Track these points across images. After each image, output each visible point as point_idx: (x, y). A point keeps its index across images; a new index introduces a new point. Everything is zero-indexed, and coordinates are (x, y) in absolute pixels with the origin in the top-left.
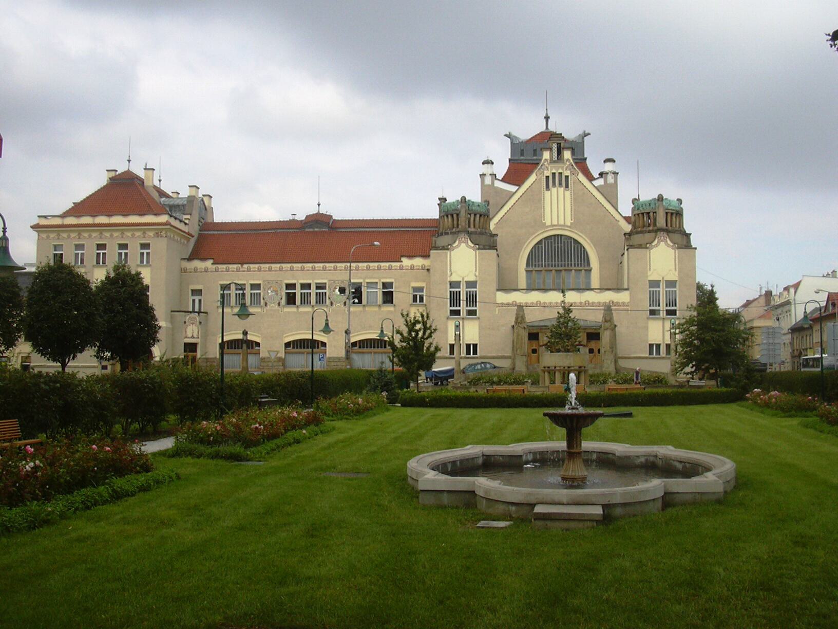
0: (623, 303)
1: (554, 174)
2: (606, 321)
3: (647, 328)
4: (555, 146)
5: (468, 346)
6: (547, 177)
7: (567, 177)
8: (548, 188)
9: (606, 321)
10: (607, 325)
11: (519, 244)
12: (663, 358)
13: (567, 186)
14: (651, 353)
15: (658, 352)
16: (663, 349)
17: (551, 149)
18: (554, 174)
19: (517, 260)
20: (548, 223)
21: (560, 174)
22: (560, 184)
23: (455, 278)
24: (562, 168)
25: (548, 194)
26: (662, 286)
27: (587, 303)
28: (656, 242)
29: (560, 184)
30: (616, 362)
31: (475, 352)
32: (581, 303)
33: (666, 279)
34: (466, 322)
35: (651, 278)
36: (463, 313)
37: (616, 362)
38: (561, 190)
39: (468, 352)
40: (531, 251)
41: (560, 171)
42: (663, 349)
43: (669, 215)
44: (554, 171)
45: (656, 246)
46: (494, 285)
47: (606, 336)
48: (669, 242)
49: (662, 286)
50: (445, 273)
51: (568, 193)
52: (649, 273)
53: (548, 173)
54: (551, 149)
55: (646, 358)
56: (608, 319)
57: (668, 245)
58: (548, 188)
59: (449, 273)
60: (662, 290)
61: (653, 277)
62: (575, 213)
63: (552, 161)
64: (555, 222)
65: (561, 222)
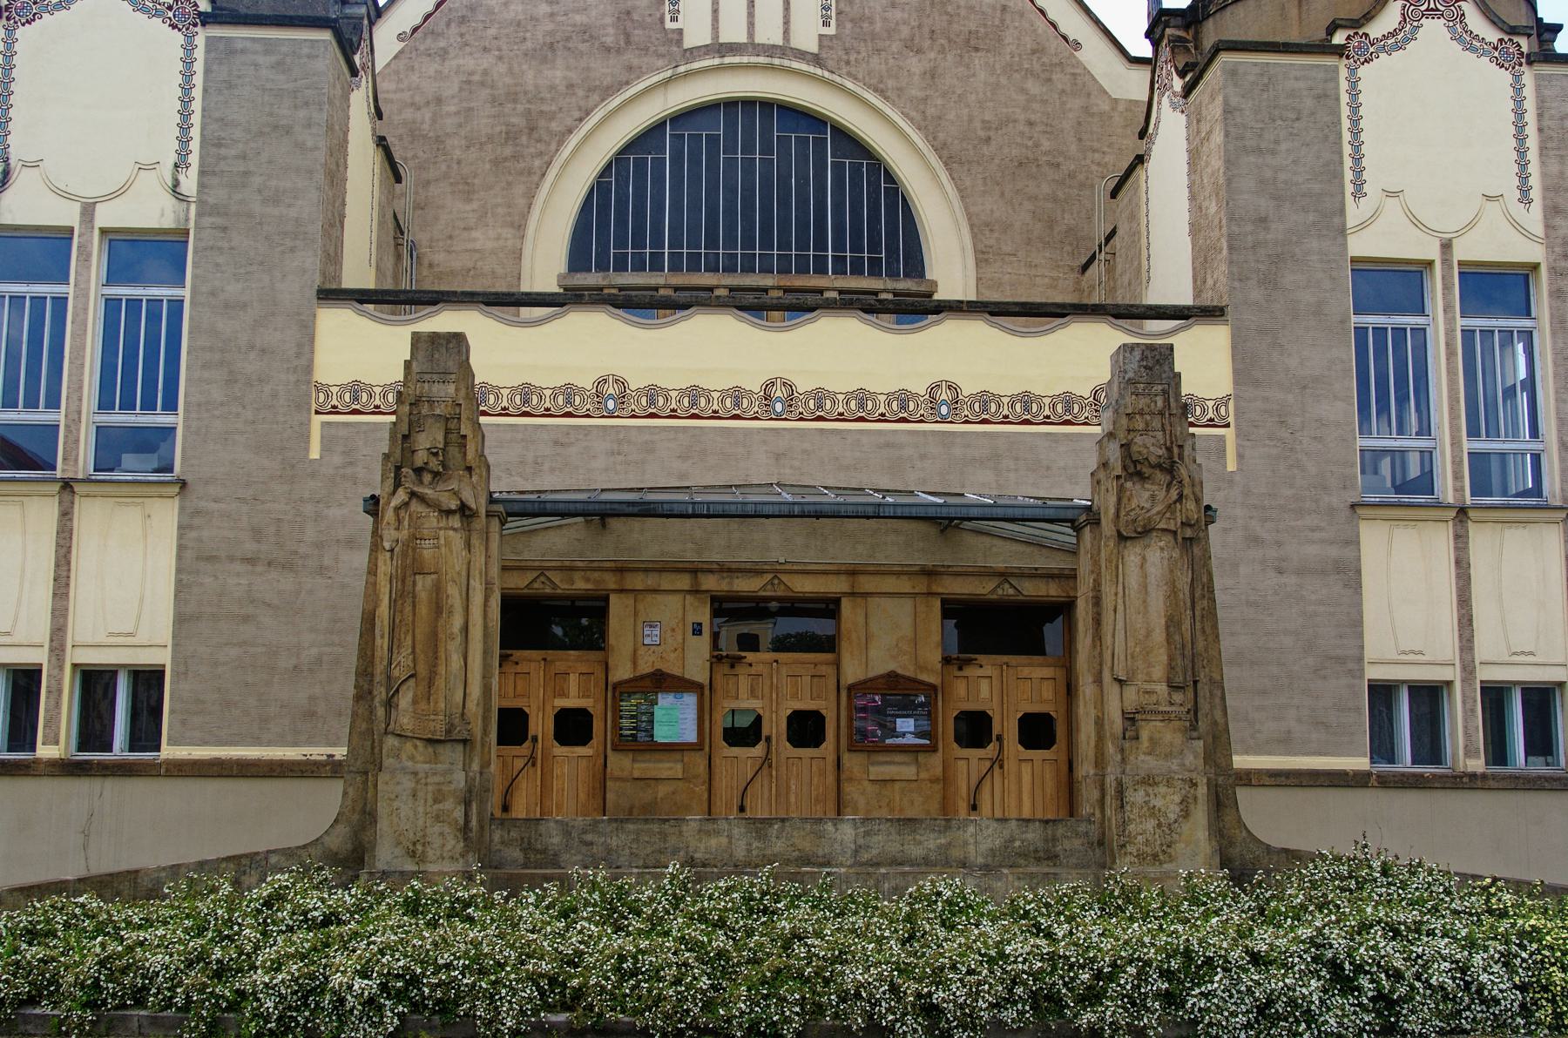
2: (1135, 469)
3: (1350, 575)
9: (1135, 469)
10: (1146, 498)
12: (1468, 782)
14: (1382, 747)
15: (1430, 744)
16: (1463, 728)
19: (520, 227)
20: (697, 33)
26: (1441, 294)
27: (943, 401)
30: (1221, 802)
31: (146, 732)
33: (1466, 251)
34: (91, 514)
35: (1361, 245)
37: (1221, 802)
39: (93, 731)
40: (600, 188)
42: (1463, 728)
45: (1397, 40)
47: (1133, 595)
48: (1475, 21)
49: (1441, 294)
52: (1354, 213)
56: (1150, 446)
57: (1469, 42)
60: (1442, 320)
61: (1378, 235)
64: (734, 32)
65: (769, 33)
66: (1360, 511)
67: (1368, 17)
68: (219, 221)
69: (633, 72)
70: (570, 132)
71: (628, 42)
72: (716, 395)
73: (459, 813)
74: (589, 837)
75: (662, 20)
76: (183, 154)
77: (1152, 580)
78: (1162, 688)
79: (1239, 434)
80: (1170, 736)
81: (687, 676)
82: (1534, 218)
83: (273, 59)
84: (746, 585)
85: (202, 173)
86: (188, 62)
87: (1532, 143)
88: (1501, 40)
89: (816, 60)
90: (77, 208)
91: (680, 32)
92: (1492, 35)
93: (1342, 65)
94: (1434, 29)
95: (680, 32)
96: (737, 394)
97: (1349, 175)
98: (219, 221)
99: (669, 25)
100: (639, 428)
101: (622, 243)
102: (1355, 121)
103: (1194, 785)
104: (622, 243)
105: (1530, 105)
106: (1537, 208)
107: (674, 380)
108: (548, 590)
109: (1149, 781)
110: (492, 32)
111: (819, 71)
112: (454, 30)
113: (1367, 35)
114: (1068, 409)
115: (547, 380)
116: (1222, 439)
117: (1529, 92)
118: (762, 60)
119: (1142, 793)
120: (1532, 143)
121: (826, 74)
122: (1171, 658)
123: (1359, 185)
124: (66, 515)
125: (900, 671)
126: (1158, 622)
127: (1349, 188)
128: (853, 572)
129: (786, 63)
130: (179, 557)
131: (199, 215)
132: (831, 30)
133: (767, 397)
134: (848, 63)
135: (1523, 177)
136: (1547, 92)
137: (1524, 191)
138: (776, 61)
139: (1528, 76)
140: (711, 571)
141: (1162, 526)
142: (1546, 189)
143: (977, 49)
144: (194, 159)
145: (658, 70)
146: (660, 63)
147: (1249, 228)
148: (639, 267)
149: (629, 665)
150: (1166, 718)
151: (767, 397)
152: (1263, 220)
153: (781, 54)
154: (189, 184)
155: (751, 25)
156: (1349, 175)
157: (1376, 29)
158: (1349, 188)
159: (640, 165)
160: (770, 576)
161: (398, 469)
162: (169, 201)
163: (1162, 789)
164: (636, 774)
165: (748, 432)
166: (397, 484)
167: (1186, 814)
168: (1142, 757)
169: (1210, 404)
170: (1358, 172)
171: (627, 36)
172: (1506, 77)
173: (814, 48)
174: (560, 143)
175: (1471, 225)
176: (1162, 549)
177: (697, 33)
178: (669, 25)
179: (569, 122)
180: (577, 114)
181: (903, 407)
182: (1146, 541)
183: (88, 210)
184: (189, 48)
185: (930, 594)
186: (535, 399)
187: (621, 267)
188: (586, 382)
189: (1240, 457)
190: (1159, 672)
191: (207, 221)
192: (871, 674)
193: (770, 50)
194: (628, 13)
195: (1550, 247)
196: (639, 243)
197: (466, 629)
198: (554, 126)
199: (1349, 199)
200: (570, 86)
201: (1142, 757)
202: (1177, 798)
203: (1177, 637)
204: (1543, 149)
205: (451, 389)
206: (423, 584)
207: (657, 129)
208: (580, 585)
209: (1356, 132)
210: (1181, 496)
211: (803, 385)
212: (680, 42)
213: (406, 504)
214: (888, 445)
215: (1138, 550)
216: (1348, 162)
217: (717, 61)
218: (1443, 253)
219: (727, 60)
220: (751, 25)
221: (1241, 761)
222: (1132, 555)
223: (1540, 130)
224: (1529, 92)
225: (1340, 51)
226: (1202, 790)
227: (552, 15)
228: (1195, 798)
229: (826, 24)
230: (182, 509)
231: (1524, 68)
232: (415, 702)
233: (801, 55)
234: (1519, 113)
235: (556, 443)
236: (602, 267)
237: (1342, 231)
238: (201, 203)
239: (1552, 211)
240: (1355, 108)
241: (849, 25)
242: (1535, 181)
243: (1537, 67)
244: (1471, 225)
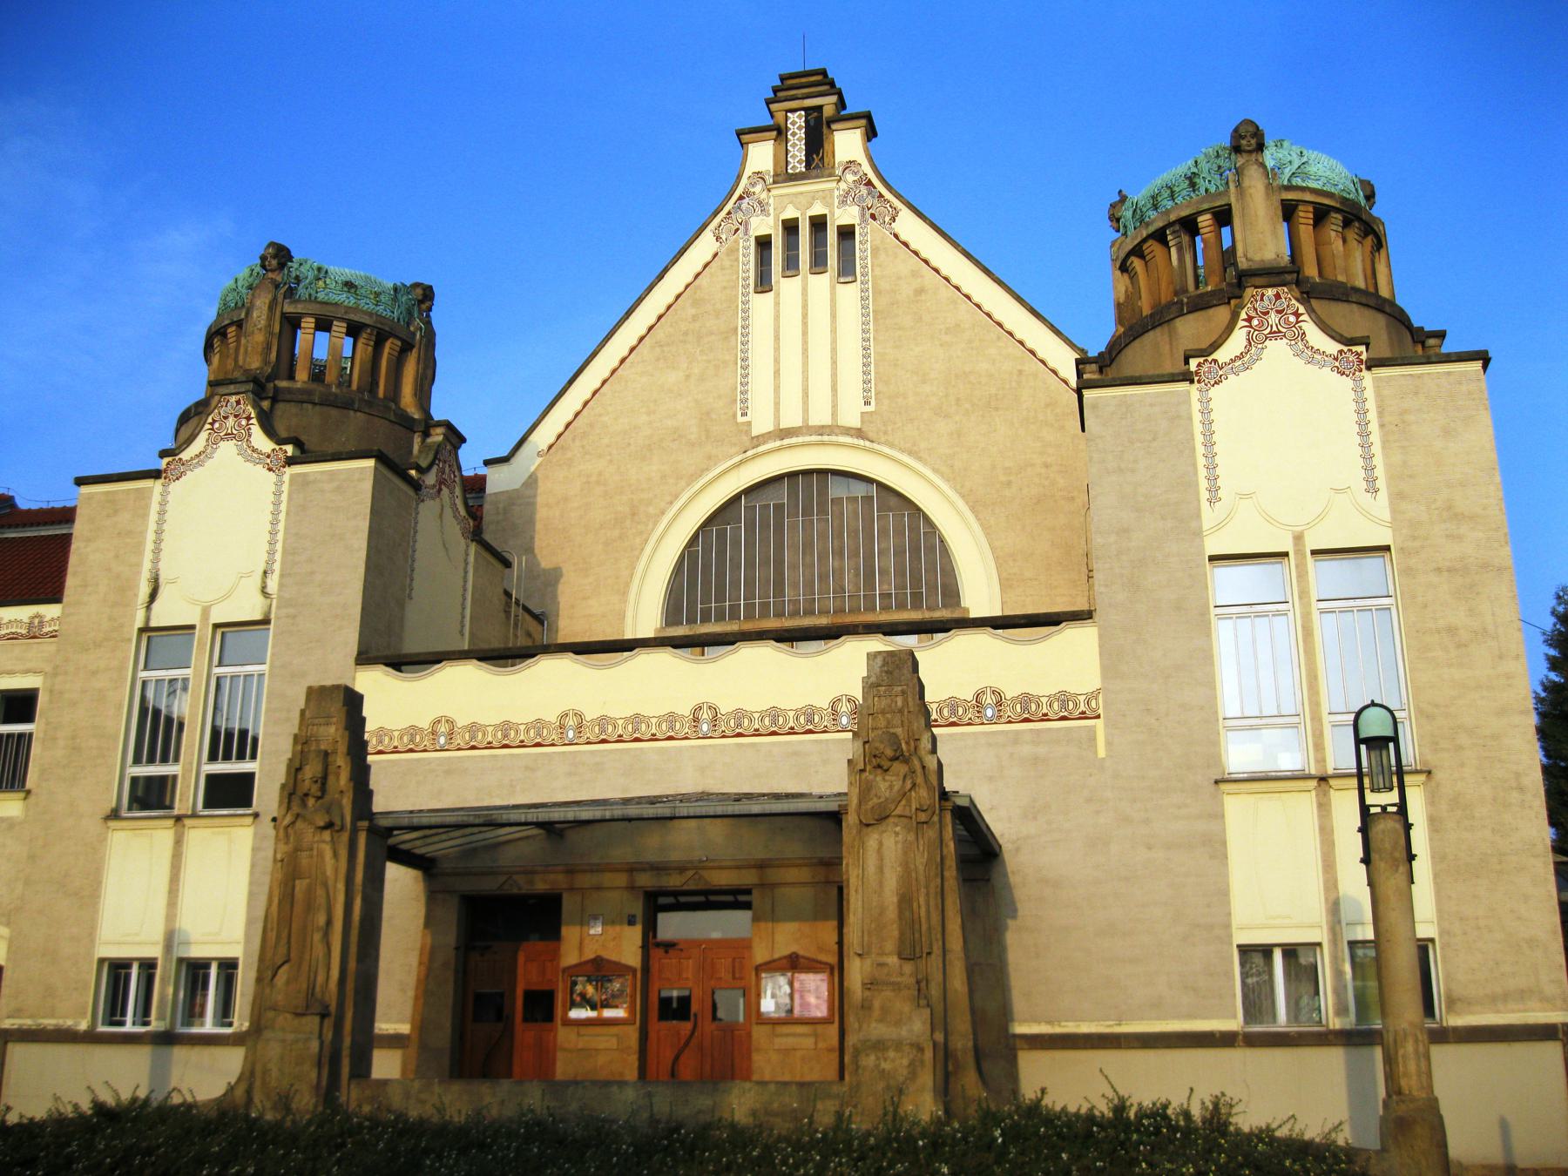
0: (1064, 698)
1: (790, 228)
3: (1216, 847)
4: (797, 122)
5: (195, 971)
6: (764, 243)
7: (846, 233)
8: (764, 283)
10: (886, 786)
11: (633, 524)
13: (847, 269)
17: (780, 132)
18: (790, 228)
19: (624, 593)
21: (819, 224)
22: (819, 263)
23: (166, 613)
24: (826, 197)
25: (761, 304)
28: (1237, 341)
29: (819, 263)
32: (810, 713)
36: (189, 794)
38: (821, 284)
41: (818, 209)
43: (1305, 216)
44: (790, 213)
45: (1242, 361)
46: (349, 638)
50: (125, 588)
51: (849, 294)
53: (766, 225)
54: (780, 132)
55: (1225, 1040)
57: (1312, 355)
58: (764, 283)
59: (144, 590)
62: (878, 377)
63: (784, 176)
64: (791, 419)
65: (820, 417)
66: (1224, 787)
67: (1215, 346)
68: (291, 611)
69: (712, 460)
70: (663, 513)
71: (708, 437)
72: (654, 721)
73: (314, 1075)
74: (423, 1096)
75: (735, 416)
76: (270, 562)
77: (887, 862)
78: (893, 960)
79: (1106, 725)
80: (903, 1006)
81: (623, 961)
82: (1381, 505)
83: (335, 484)
84: (674, 881)
85: (282, 576)
86: (278, 494)
87: (1375, 438)
88: (1341, 352)
89: (859, 433)
90: (198, 610)
91: (749, 423)
92: (1333, 347)
93: (1194, 390)
94: (1277, 350)
95: (749, 423)
96: (671, 718)
97: (1203, 485)
98: (291, 611)
99: (740, 419)
100: (592, 752)
101: (706, 599)
102: (1208, 434)
103: (921, 1049)
104: (706, 599)
105: (1371, 405)
106: (1383, 495)
107: (620, 710)
108: (515, 891)
109: (879, 1046)
110: (606, 441)
111: (861, 442)
112: (578, 443)
113: (1215, 361)
114: (954, 711)
115: (522, 716)
116: (1092, 730)
117: (1369, 394)
118: (815, 438)
119: (873, 1057)
120: (1375, 438)
121: (867, 444)
122: (902, 934)
123: (1214, 490)
124: (178, 842)
125: (801, 953)
126: (891, 898)
127: (1204, 495)
128: (762, 866)
129: (833, 438)
130: (252, 873)
131: (278, 607)
132: (871, 408)
133: (696, 720)
134: (885, 433)
135: (1369, 469)
136: (1385, 392)
137: (1371, 482)
138: (826, 438)
139: (1368, 377)
140: (644, 870)
141: (897, 812)
142: (1391, 478)
143: (997, 409)
144: (277, 566)
145: (731, 457)
146: (734, 450)
147: (1113, 538)
148: (720, 617)
149: (576, 953)
150: (897, 987)
151: (696, 720)
152: (1124, 531)
153: (827, 432)
154: (273, 585)
155: (806, 411)
156: (1203, 485)
157: (1222, 355)
158: (1204, 495)
159: (722, 536)
160: (691, 873)
161: (290, 795)
162: (260, 598)
163: (891, 1054)
164: (580, 1045)
165: (680, 749)
166: (289, 808)
167: (913, 1075)
168: (874, 1025)
169: (1082, 698)
170: (1213, 478)
171: (707, 431)
172: (1347, 382)
173: (856, 423)
174: (655, 524)
175: (1321, 517)
176: (897, 834)
177: (762, 422)
178: (740, 419)
179: (663, 505)
180: (668, 499)
181: (810, 721)
182: (883, 827)
183: (206, 612)
184: (279, 484)
185: (827, 882)
186: (512, 733)
187: (706, 618)
188: (552, 717)
189: (1109, 744)
190: (890, 946)
191: (284, 611)
192: (776, 956)
193: (820, 430)
194: (708, 414)
195: (1396, 530)
196: (720, 598)
197: (329, 922)
198: (651, 510)
199: (1204, 505)
200: (664, 477)
201: (874, 1025)
202: (905, 1062)
203: (907, 914)
204: (1385, 444)
205: (332, 729)
206: (301, 886)
207: (735, 499)
208: (541, 886)
209: (1209, 444)
210: (914, 785)
211: (725, 708)
212: (748, 432)
213: (293, 823)
214: (796, 754)
215: (876, 836)
216: (1202, 473)
217: (778, 443)
218: (1295, 545)
219: (786, 442)
220: (806, 411)
221: (1020, 1029)
222: (872, 840)
223: (1382, 426)
224: (1369, 394)
225: (1188, 377)
226: (929, 1054)
227: (650, 423)
228: (922, 1062)
229: (867, 403)
230: (255, 835)
231: (1365, 373)
232: (288, 982)
233: (847, 431)
234: (1362, 412)
235: (527, 768)
236: (691, 621)
237: (1198, 534)
238: (279, 597)
239: (1397, 497)
240: (1208, 423)
241: (886, 402)
242: (1380, 472)
243: (1375, 370)
244: (1321, 517)
